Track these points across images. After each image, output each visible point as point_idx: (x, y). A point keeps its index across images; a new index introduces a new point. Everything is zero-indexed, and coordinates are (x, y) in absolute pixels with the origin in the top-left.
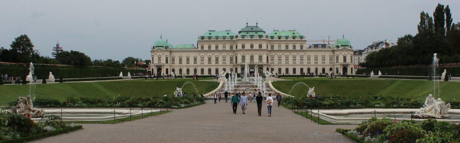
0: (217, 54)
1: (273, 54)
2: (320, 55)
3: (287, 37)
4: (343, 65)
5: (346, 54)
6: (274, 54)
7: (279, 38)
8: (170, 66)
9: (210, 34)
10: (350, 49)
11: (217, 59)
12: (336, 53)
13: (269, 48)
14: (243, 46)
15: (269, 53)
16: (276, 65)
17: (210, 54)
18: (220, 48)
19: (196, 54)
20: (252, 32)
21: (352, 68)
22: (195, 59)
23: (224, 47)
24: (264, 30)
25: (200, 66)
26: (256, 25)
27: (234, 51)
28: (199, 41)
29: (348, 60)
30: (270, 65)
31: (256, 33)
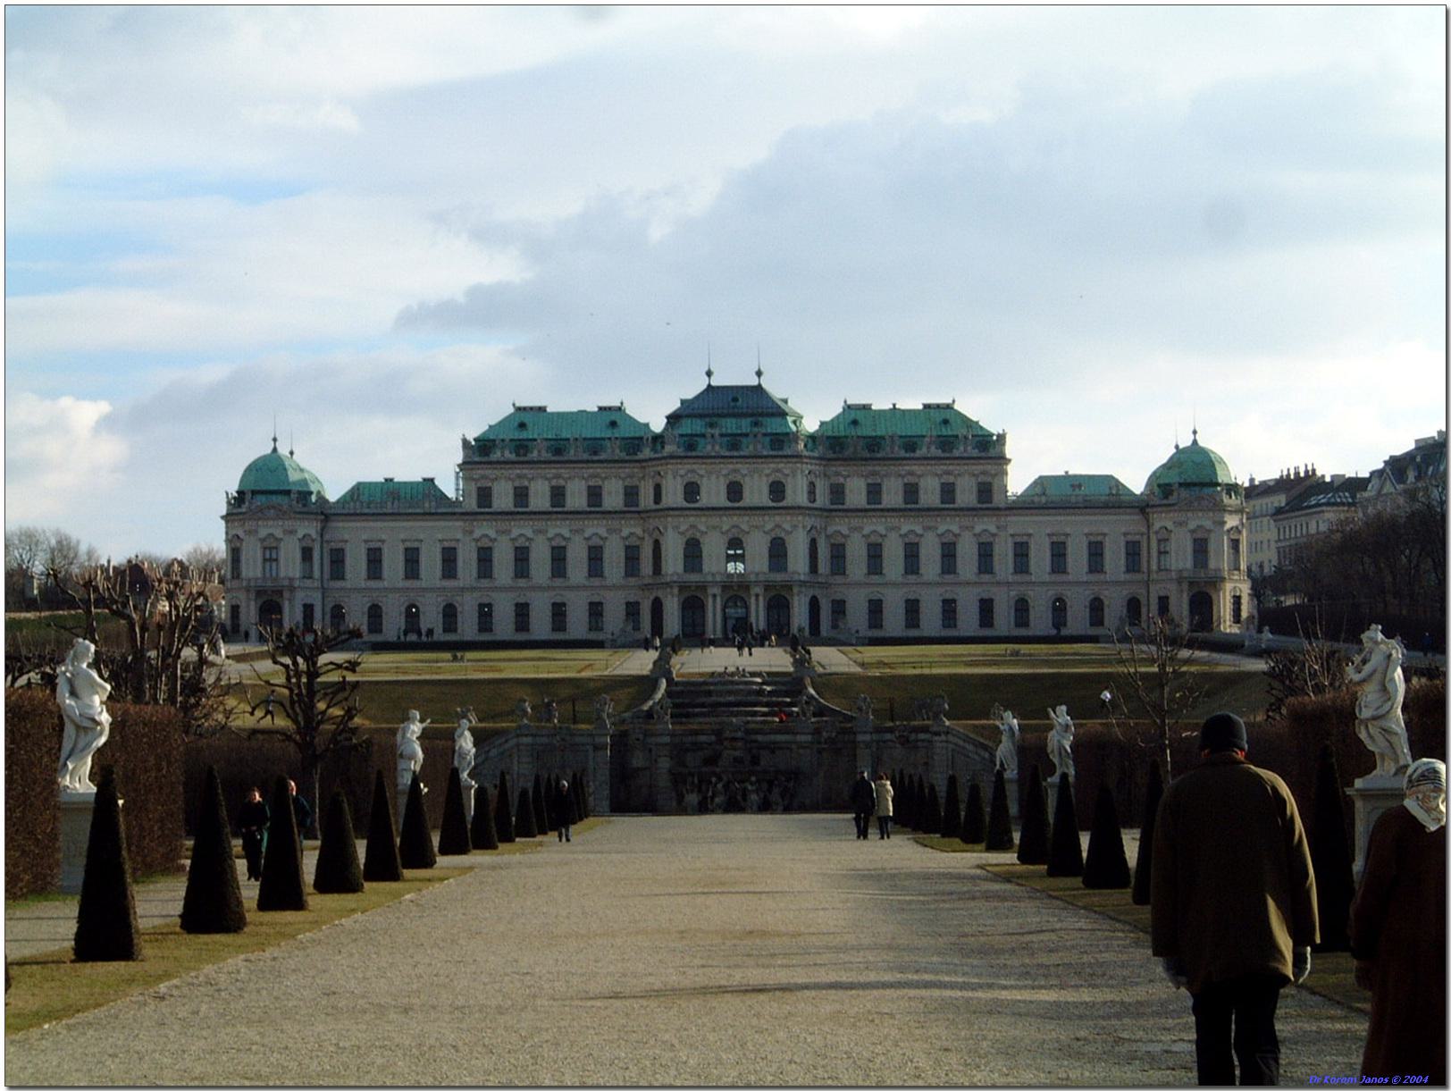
1: (840, 526)
3: (911, 444)
5: (1208, 524)
6: (845, 531)
8: (324, 590)
9: (522, 426)
13: (822, 499)
14: (692, 491)
15: (818, 523)
16: (859, 584)
19: (451, 530)
21: (1237, 600)
24: (794, 405)
25: (473, 589)
26: (755, 383)
27: (643, 514)
29: (1221, 558)
31: (756, 424)
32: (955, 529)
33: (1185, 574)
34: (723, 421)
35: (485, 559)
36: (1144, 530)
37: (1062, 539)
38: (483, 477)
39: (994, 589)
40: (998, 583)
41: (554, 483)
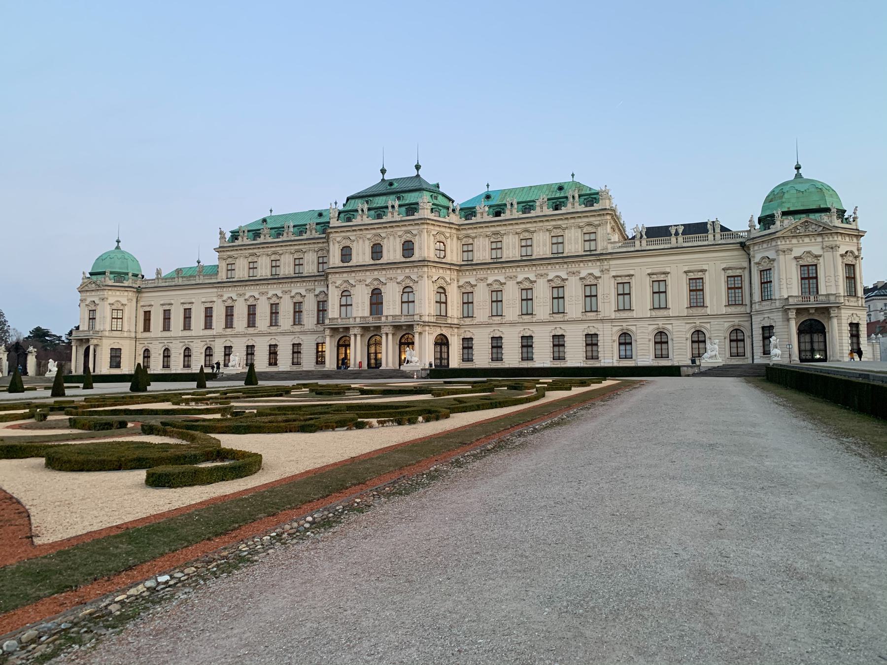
0: (274, 290)
2: (677, 269)
3: (527, 207)
4: (799, 311)
5: (817, 250)
9: (264, 220)
10: (837, 223)
13: (454, 255)
14: (346, 253)
15: (448, 275)
17: (251, 292)
20: (397, 198)
21: (854, 327)
23: (298, 264)
25: (221, 336)
26: (414, 173)
28: (220, 249)
30: (451, 326)
32: (564, 276)
33: (791, 301)
34: (377, 198)
36: (746, 264)
37: (662, 277)
38: (230, 257)
39: (598, 325)
40: (602, 320)
41: (273, 257)
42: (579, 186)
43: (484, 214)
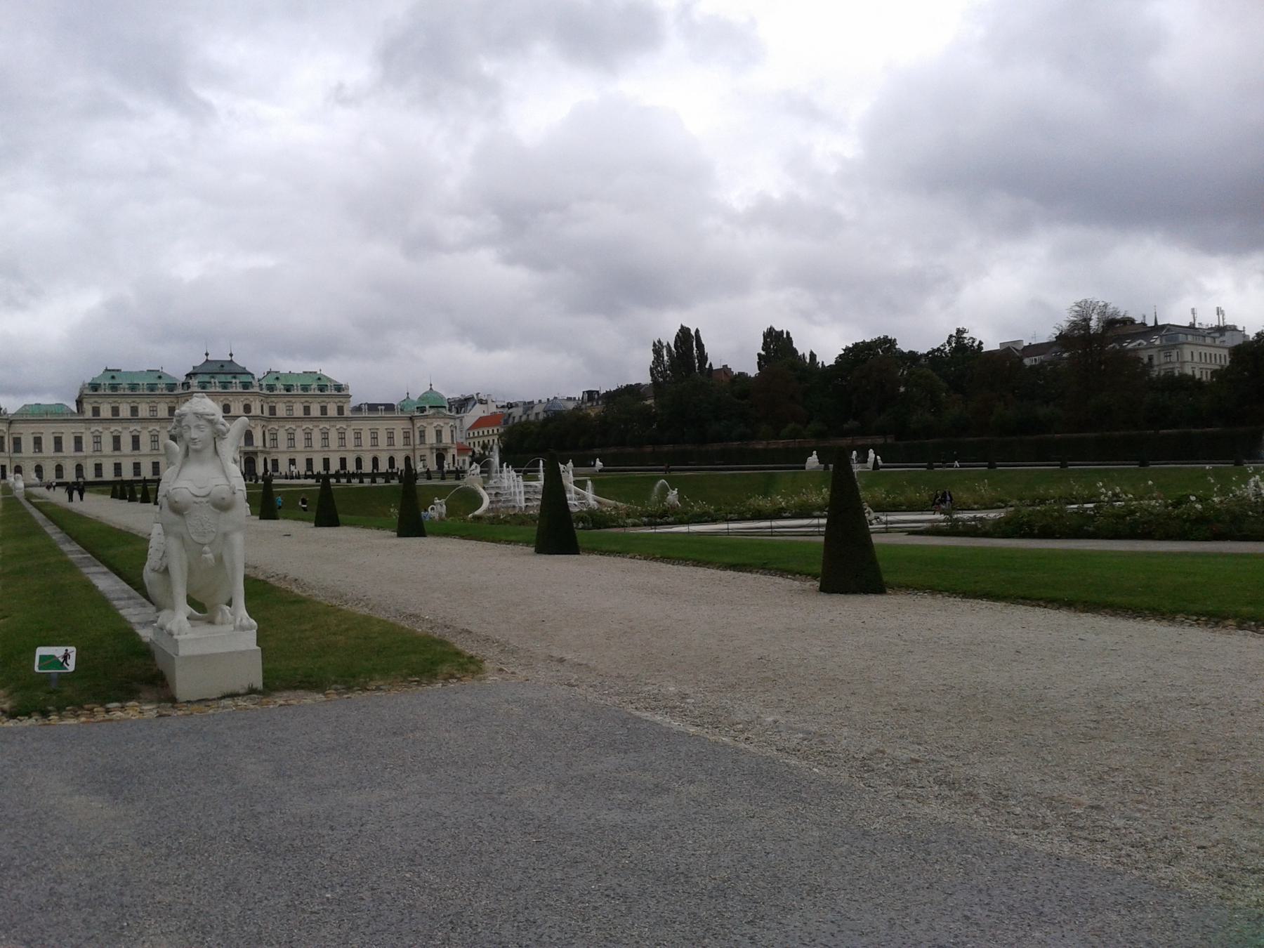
0: (135, 427)
1: (274, 425)
2: (382, 427)
3: (305, 388)
7: (288, 390)
8: (11, 458)
9: (113, 377)
11: (136, 442)
12: (418, 424)
13: (266, 413)
18: (144, 411)
19: (80, 428)
22: (78, 442)
23: (153, 410)
29: (446, 439)
30: (268, 453)
35: (97, 441)
42: (329, 379)
43: (280, 390)
